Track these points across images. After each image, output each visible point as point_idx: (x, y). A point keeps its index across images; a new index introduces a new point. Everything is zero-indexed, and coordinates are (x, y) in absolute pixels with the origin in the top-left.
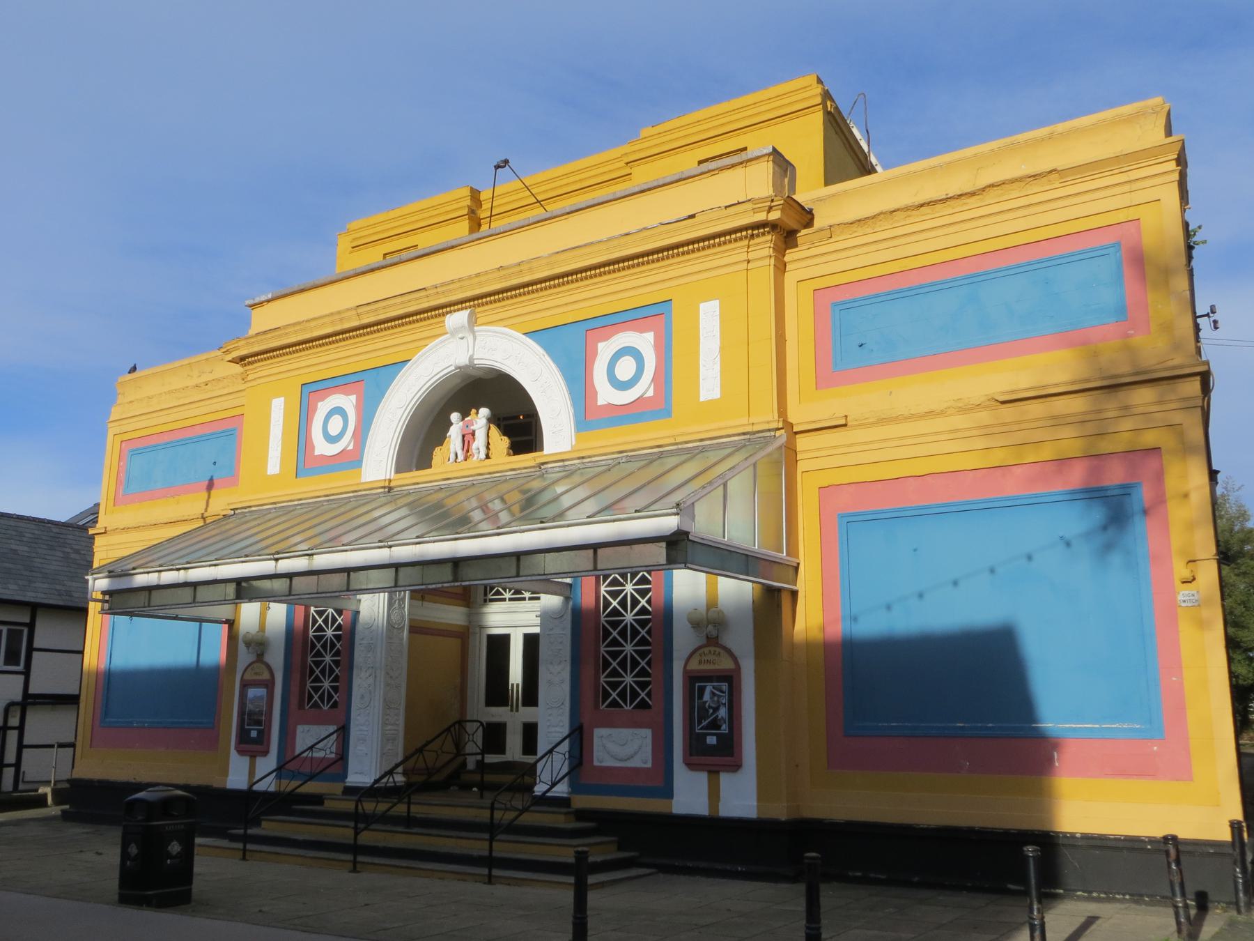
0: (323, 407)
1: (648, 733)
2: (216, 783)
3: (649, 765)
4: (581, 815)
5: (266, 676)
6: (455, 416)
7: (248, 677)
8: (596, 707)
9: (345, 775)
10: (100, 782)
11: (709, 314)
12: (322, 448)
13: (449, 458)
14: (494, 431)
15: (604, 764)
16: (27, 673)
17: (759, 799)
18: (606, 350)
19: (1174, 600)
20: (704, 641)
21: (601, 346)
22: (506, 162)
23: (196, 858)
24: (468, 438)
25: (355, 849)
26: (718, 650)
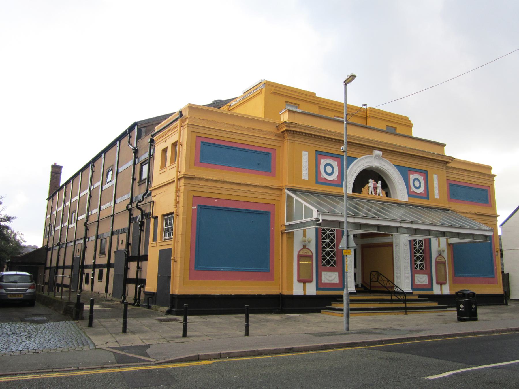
2: (286, 292)
5: (310, 254)
10: (202, 296)
24: (376, 188)
25: (406, 309)
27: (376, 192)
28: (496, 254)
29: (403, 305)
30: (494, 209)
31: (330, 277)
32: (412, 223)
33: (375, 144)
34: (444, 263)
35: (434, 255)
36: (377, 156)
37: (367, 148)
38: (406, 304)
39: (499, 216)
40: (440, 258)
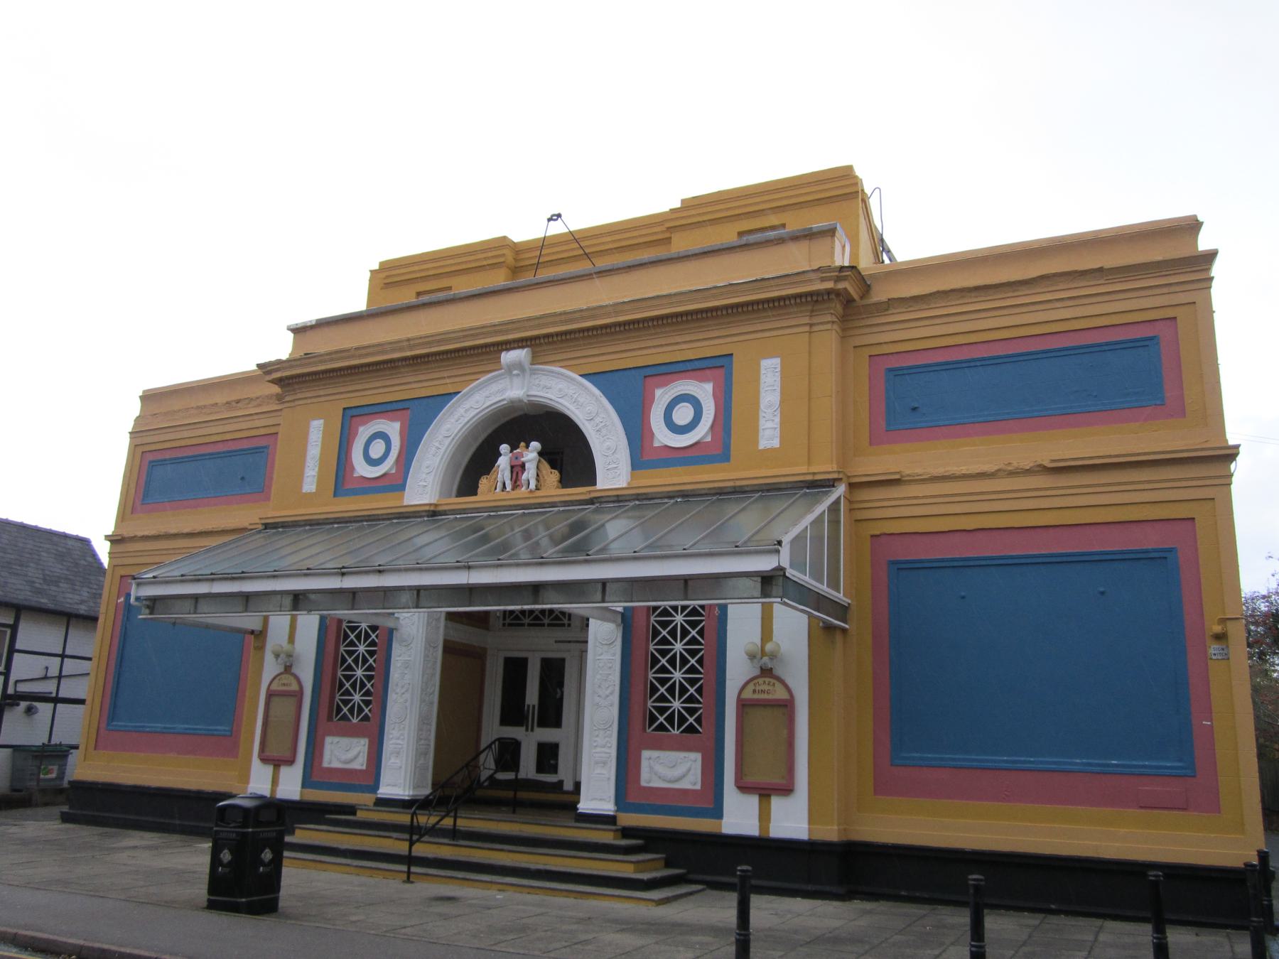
0: (364, 432)
1: (697, 756)
3: (698, 787)
4: (627, 832)
5: (295, 687)
6: (504, 448)
7: (275, 687)
8: (644, 730)
9: (378, 788)
11: (770, 373)
12: (362, 469)
13: (496, 486)
14: (546, 466)
15: (652, 785)
16: (7, 674)
17: (810, 823)
18: (662, 396)
19: (1206, 652)
20: (757, 672)
21: (658, 392)
22: (559, 216)
23: (284, 870)
24: (517, 469)
26: (772, 681)
27: (516, 484)
28: (1213, 649)
29: (401, 847)
30: (1213, 414)
31: (345, 752)
32: (380, 572)
33: (497, 333)
34: (787, 706)
35: (737, 671)
36: (519, 366)
37: (479, 354)
38: (412, 844)
39: (1237, 447)
40: (764, 684)
